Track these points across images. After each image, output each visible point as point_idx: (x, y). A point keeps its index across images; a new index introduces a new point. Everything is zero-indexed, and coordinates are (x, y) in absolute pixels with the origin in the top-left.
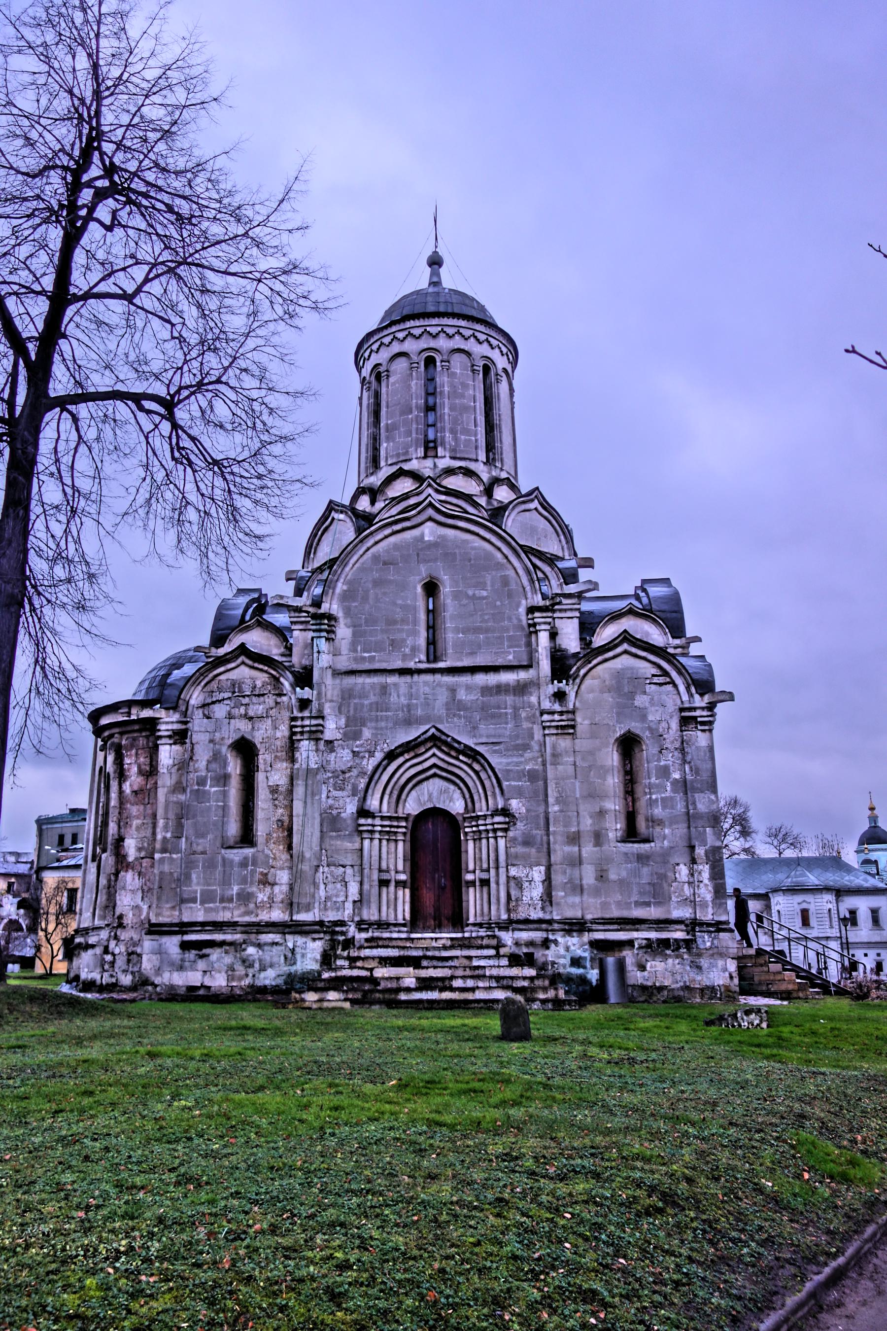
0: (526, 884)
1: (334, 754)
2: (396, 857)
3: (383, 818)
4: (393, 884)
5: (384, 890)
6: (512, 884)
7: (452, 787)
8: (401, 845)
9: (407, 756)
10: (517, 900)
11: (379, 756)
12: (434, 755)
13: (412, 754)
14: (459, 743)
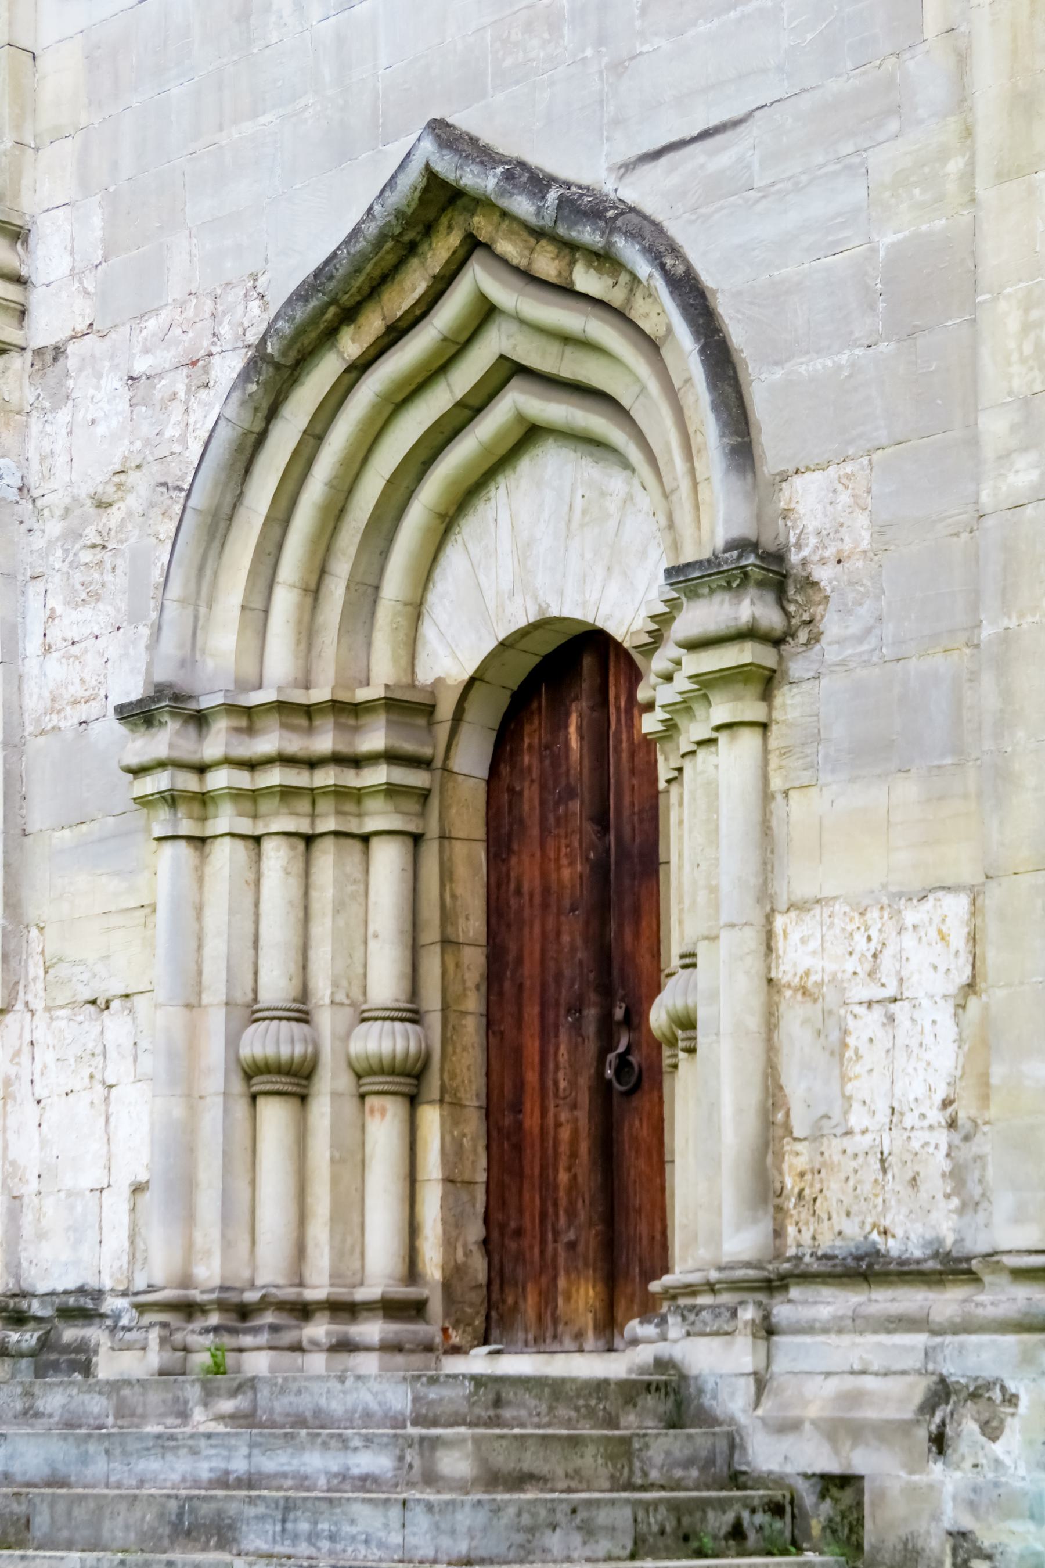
0: (866, 1026)
1: (63, 416)
2: (362, 930)
3: (249, 718)
4: (331, 1084)
5: (274, 1115)
6: (795, 1019)
7: (616, 482)
8: (388, 860)
9: (351, 345)
10: (816, 1137)
11: (228, 367)
12: (486, 312)
13: (373, 324)
14: (538, 182)
